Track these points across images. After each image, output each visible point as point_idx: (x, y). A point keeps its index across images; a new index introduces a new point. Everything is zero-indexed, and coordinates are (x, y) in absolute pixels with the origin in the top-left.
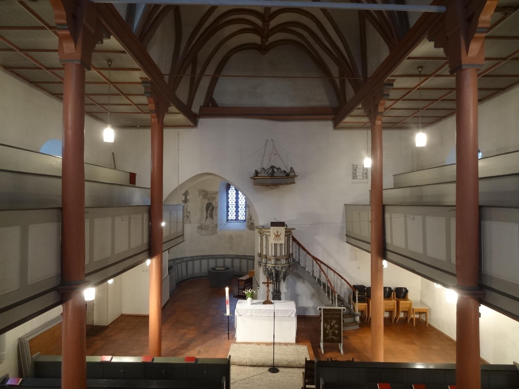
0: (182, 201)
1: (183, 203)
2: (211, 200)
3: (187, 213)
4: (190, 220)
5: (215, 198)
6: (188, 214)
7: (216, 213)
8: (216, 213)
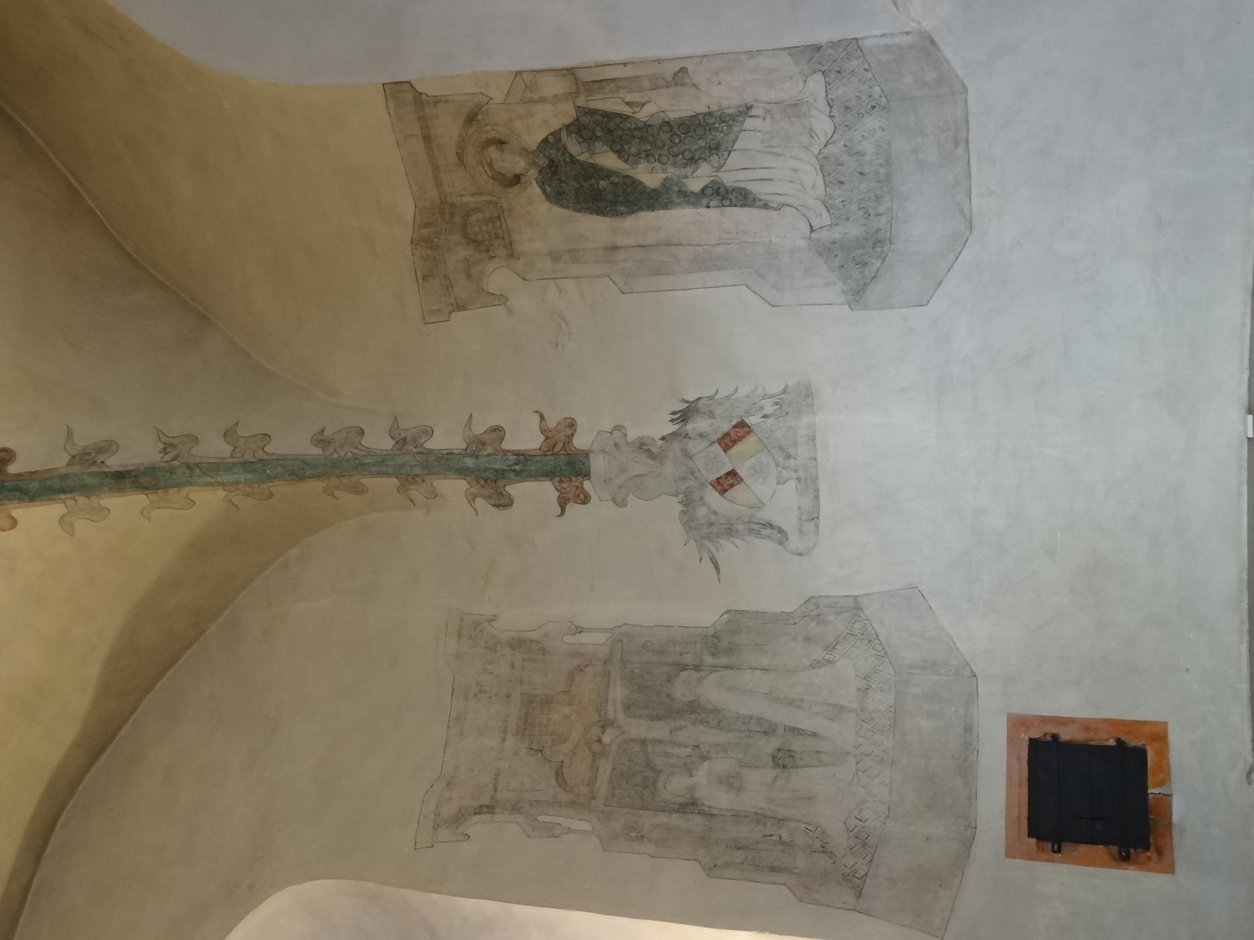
0: (563, 504)
1: (585, 499)
2: (513, 163)
3: (695, 446)
4: (768, 410)
5: (471, 119)
6: (699, 424)
7: (656, 84)
8: (656, 84)
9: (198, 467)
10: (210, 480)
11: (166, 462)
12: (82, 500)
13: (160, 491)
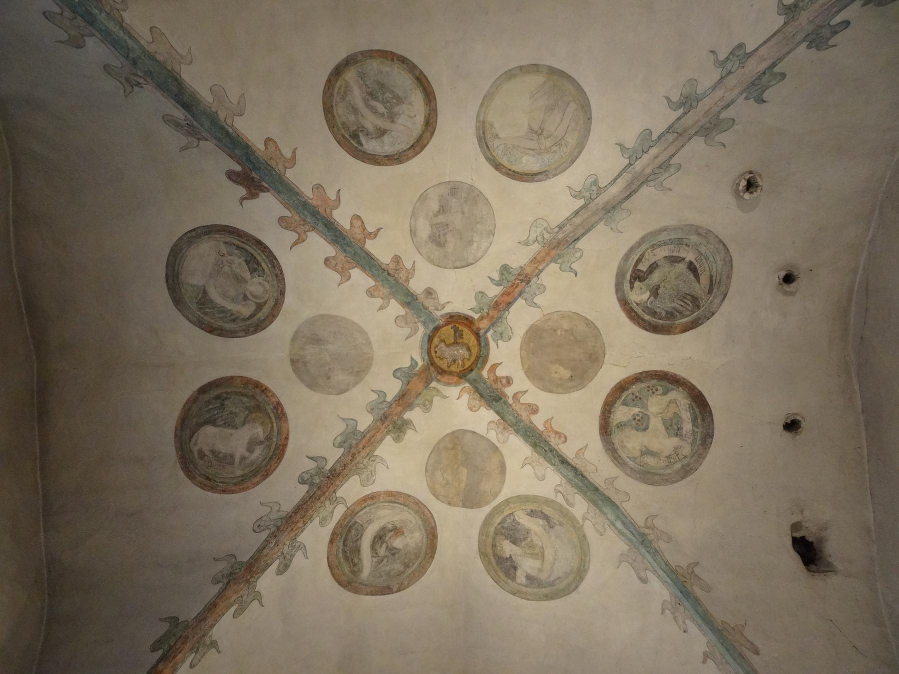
9: (127, 57)
10: (129, 41)
11: (145, 80)
12: (222, 116)
13: (169, 68)
